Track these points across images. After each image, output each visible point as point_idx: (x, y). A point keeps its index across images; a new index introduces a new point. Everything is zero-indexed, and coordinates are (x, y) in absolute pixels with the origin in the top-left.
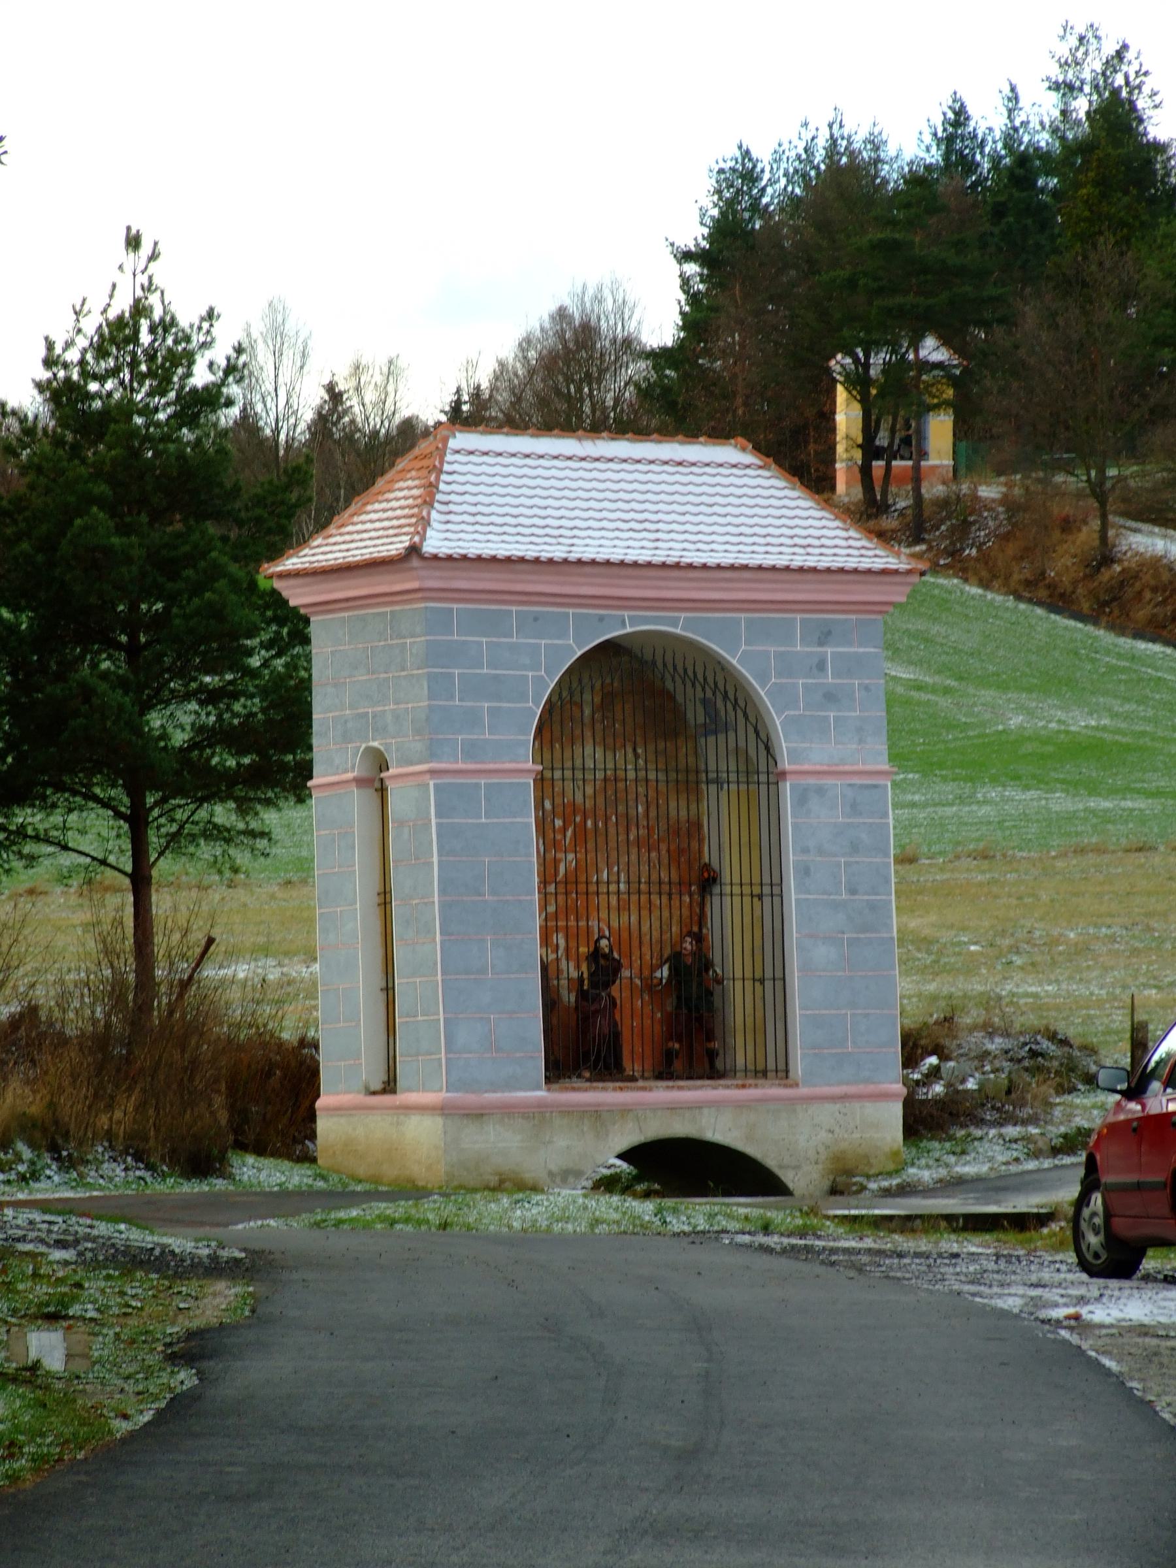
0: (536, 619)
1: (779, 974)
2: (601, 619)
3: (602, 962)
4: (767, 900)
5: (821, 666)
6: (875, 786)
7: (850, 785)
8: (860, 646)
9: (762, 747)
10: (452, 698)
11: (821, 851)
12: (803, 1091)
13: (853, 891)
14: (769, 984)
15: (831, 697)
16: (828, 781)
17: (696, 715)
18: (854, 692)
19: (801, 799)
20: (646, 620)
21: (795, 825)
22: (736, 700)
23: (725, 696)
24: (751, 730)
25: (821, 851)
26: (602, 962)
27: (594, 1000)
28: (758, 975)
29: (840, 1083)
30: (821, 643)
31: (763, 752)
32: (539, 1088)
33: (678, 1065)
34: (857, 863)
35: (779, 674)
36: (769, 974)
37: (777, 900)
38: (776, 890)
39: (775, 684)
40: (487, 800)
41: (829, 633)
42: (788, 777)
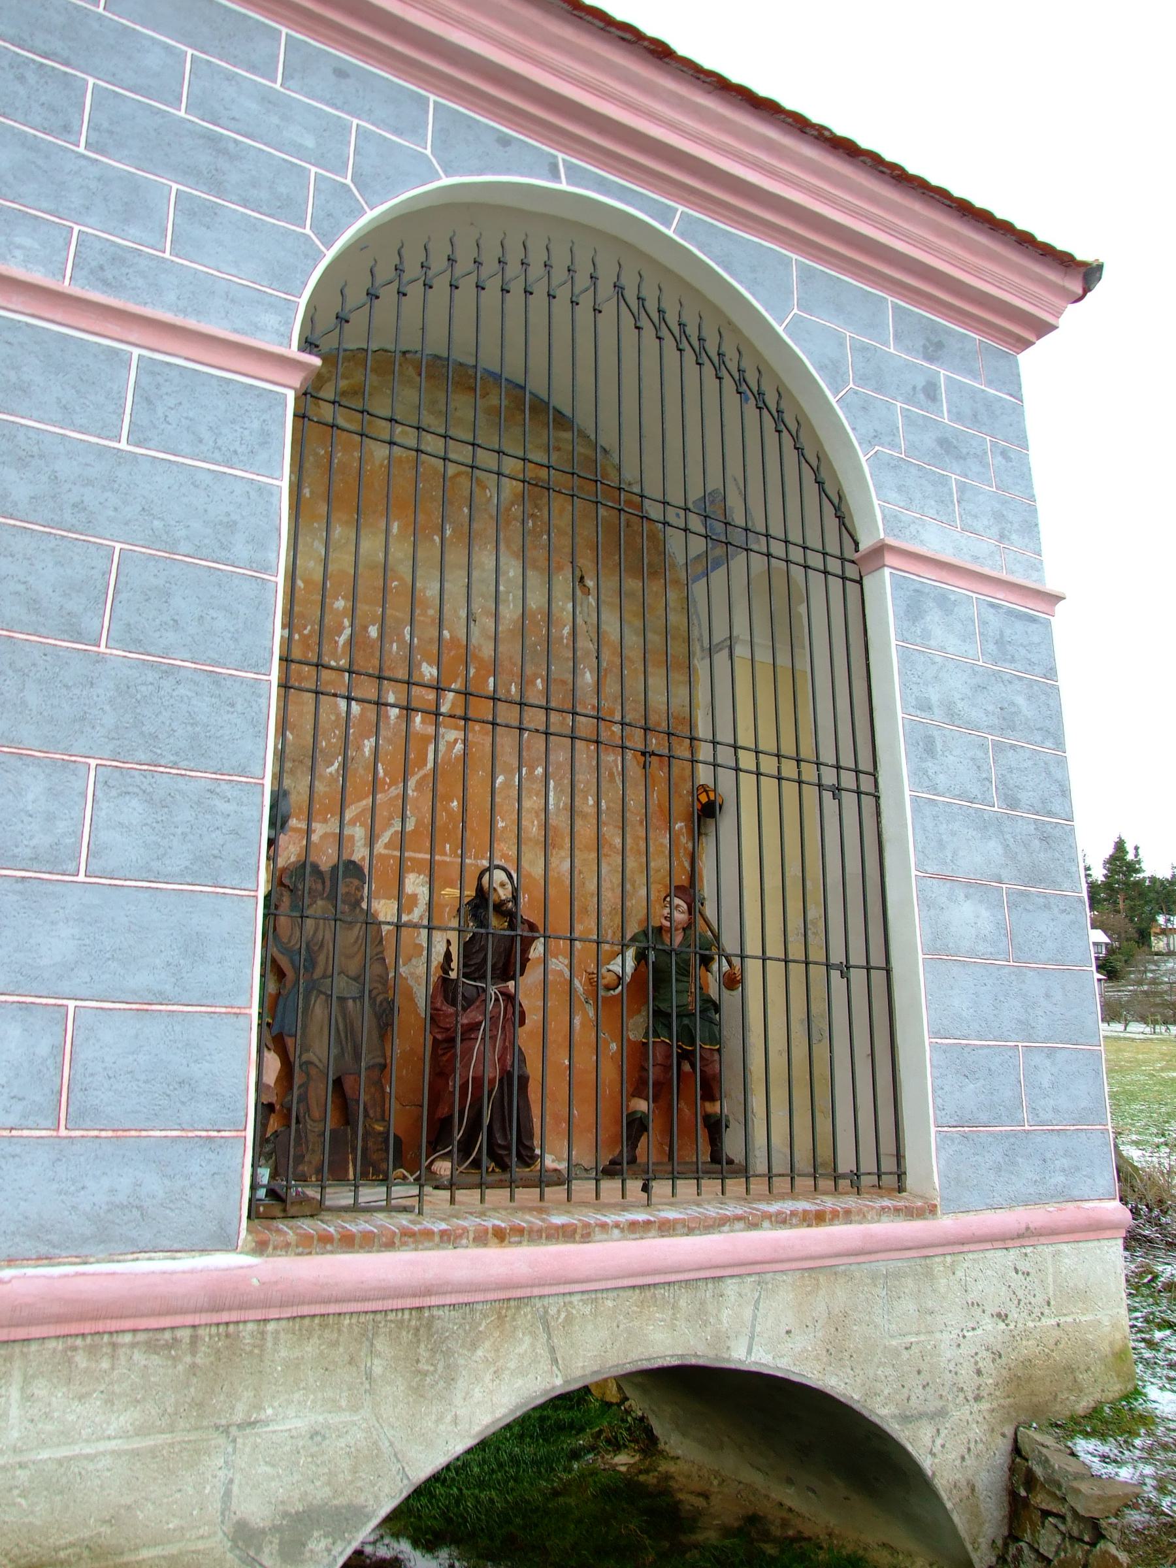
1: (877, 959)
2: (505, 141)
3: (494, 921)
4: (849, 799)
6: (1033, 620)
7: (992, 605)
8: (990, 383)
9: (829, 510)
12: (945, 1224)
13: (1012, 803)
14: (858, 976)
15: (948, 446)
16: (958, 588)
19: (913, 611)
20: (602, 186)
21: (905, 658)
24: (808, 476)
25: (951, 713)
26: (494, 921)
27: (469, 1003)
28: (837, 957)
29: (1013, 1202)
30: (930, 359)
31: (832, 523)
32: (227, 1244)
33: (649, 1148)
34: (1013, 747)
35: (862, 379)
36: (857, 958)
37: (868, 801)
38: (866, 784)
40: (145, 398)
41: (940, 345)
42: (889, 559)
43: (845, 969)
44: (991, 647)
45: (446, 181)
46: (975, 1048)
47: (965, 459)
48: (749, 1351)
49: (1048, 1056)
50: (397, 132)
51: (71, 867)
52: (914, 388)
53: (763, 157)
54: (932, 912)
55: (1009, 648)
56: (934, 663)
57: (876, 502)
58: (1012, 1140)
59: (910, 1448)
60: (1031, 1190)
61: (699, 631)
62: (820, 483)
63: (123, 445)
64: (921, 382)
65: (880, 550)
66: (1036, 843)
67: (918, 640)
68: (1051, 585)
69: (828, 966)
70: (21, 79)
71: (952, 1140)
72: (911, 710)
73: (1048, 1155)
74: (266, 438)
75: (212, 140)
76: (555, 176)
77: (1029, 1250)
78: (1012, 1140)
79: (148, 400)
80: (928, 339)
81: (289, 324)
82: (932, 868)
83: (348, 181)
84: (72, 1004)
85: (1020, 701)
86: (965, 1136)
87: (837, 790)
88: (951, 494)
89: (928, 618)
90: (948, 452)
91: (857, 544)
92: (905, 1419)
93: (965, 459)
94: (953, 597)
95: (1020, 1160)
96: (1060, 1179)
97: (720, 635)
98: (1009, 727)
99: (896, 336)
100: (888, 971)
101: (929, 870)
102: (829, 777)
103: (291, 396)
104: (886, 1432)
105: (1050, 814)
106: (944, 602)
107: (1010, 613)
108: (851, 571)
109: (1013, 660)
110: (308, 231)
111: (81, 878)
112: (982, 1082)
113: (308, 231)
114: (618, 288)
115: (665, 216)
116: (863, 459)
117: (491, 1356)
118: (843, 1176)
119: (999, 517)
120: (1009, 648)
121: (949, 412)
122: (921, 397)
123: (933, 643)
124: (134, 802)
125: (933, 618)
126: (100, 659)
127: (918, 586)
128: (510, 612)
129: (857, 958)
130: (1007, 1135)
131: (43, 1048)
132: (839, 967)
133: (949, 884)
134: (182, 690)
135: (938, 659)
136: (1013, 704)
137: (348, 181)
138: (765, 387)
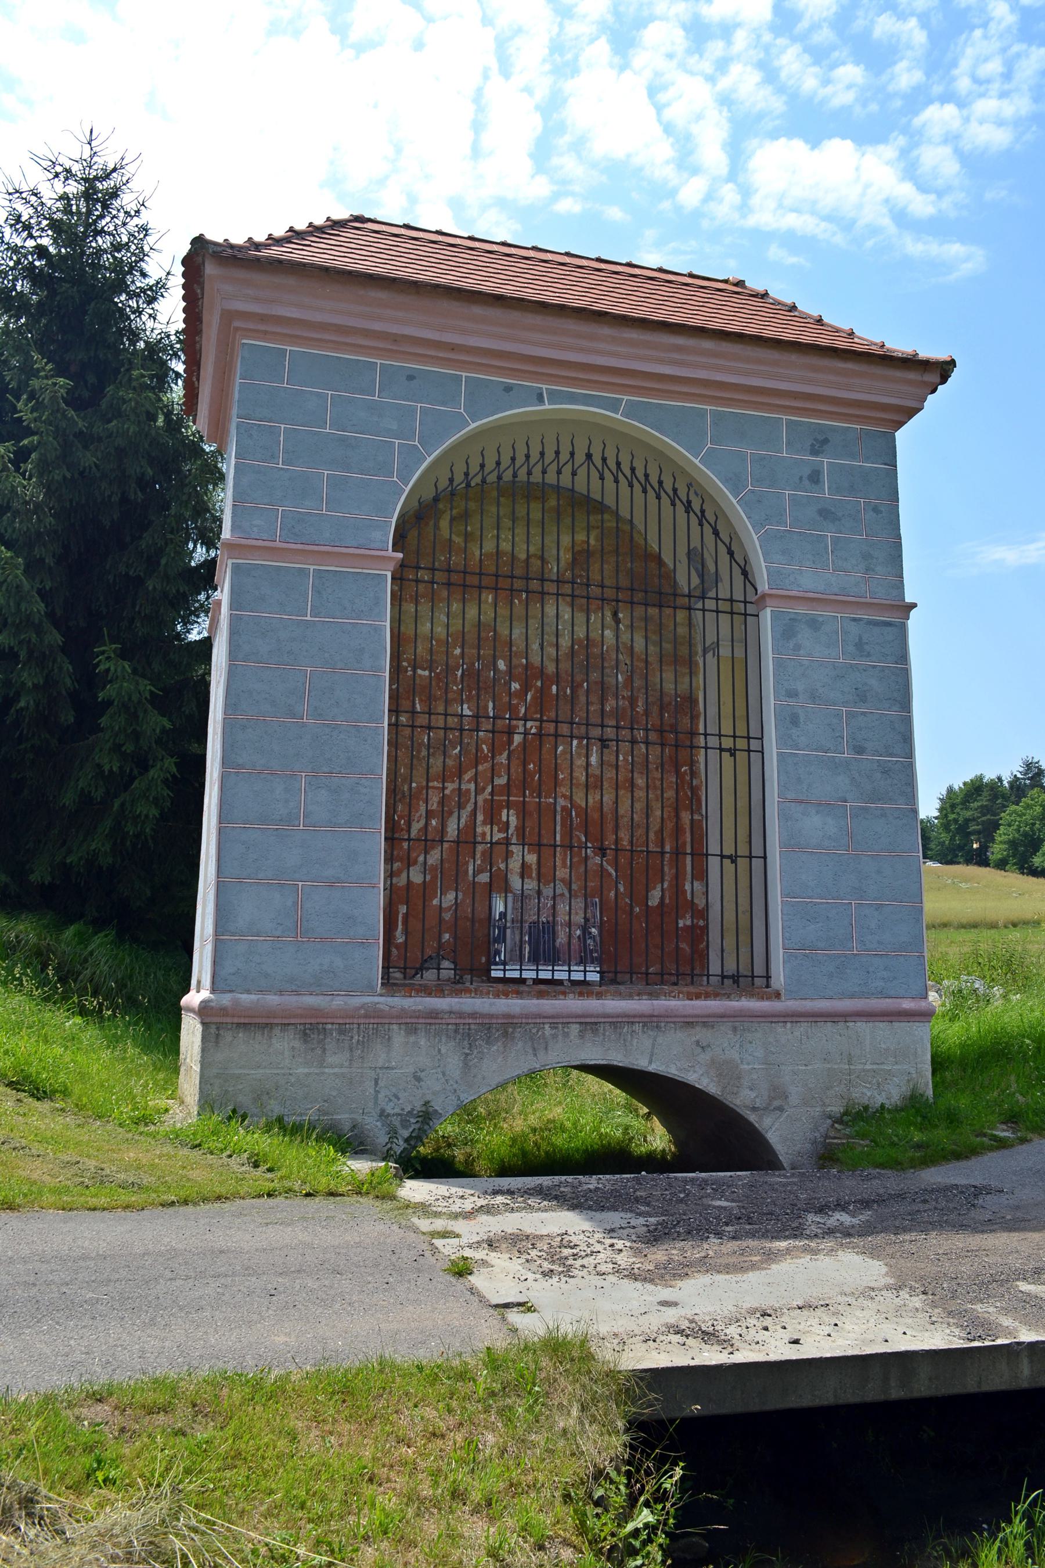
0: (411, 378)
1: (757, 851)
2: (508, 389)
4: (741, 756)
5: (815, 478)
7: (854, 620)
9: (737, 571)
10: (274, 457)
11: (813, 697)
13: (860, 750)
14: (742, 863)
17: (685, 579)
18: (859, 511)
19: (787, 631)
20: (573, 398)
21: (779, 664)
22: (703, 511)
23: (688, 507)
25: (813, 697)
29: (842, 996)
30: (815, 452)
32: (370, 989)
36: (743, 850)
38: (754, 745)
39: (752, 491)
40: (317, 591)
41: (826, 441)
42: (768, 601)
43: (734, 859)
44: (851, 648)
45: (473, 426)
46: (816, 904)
47: (840, 520)
48: (650, 1062)
49: (876, 909)
50: (443, 404)
51: (297, 823)
52: (801, 478)
53: (676, 356)
54: (789, 823)
55: (866, 647)
56: (802, 666)
57: (763, 564)
58: (843, 959)
59: (615, 1063)
60: (857, 989)
61: (698, 638)
62: (731, 553)
63: (309, 618)
64: (806, 471)
65: (764, 596)
66: (878, 775)
67: (791, 652)
68: (908, 599)
69: (722, 856)
70: (251, 436)
71: (796, 958)
72: (782, 698)
73: (871, 969)
74: (378, 601)
75: (343, 440)
76: (540, 399)
77: (851, 1024)
78: (843, 959)
79: (319, 592)
80: (815, 439)
81: (387, 535)
82: (791, 795)
83: (416, 443)
84: (300, 884)
85: (873, 682)
86: (805, 955)
87: (732, 752)
88: (826, 547)
89: (800, 636)
90: (825, 519)
91: (756, 590)
92: (754, 1109)
93: (840, 520)
94: (821, 619)
95: (848, 971)
96: (881, 984)
97: (710, 639)
98: (861, 700)
99: (788, 443)
100: (765, 858)
101: (789, 797)
102: (727, 743)
103: (389, 575)
104: (727, 1107)
105: (891, 755)
106: (814, 624)
107: (870, 623)
108: (751, 609)
109: (869, 655)
110: (395, 479)
111: (301, 827)
112: (820, 924)
113: (395, 479)
114: (589, 456)
115: (614, 406)
116: (755, 537)
117: (501, 1049)
118: (728, 977)
119: (866, 556)
120: (866, 647)
121: (829, 488)
122: (806, 482)
123: (802, 652)
124: (323, 791)
125: (804, 636)
126: (304, 725)
127: (793, 616)
128: (565, 642)
129: (743, 850)
130: (839, 956)
131: (289, 903)
132: (730, 857)
133: (803, 805)
134: (342, 736)
135: (805, 662)
136: (866, 684)
137: (416, 443)
138: (692, 497)
